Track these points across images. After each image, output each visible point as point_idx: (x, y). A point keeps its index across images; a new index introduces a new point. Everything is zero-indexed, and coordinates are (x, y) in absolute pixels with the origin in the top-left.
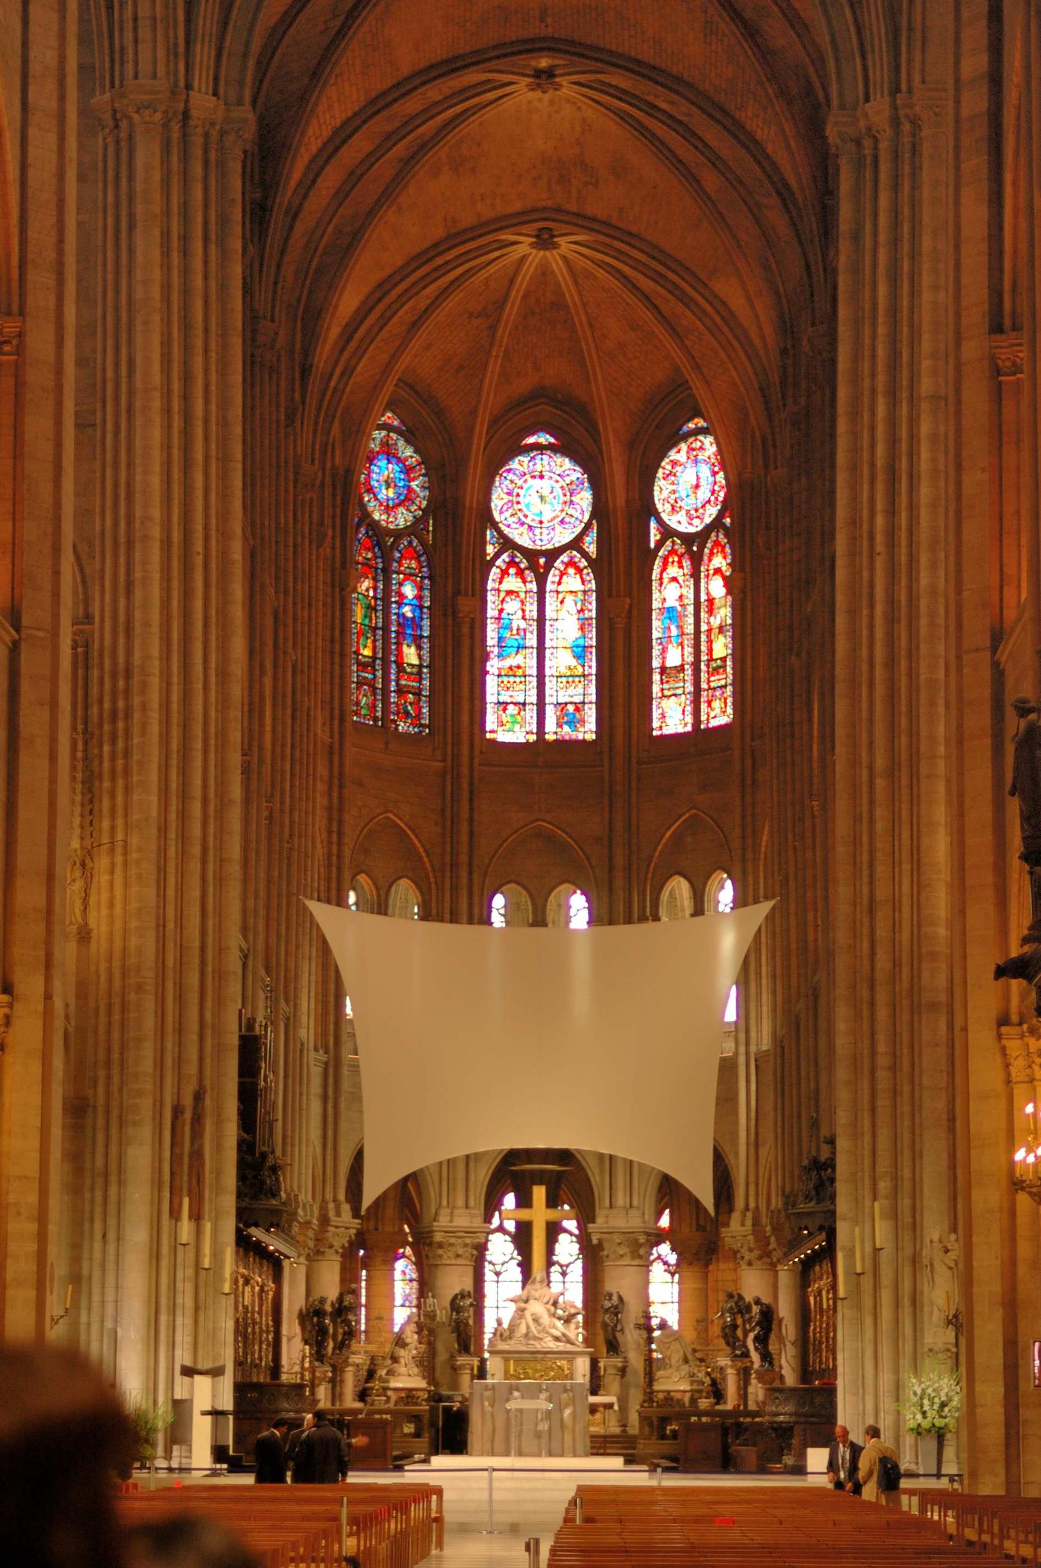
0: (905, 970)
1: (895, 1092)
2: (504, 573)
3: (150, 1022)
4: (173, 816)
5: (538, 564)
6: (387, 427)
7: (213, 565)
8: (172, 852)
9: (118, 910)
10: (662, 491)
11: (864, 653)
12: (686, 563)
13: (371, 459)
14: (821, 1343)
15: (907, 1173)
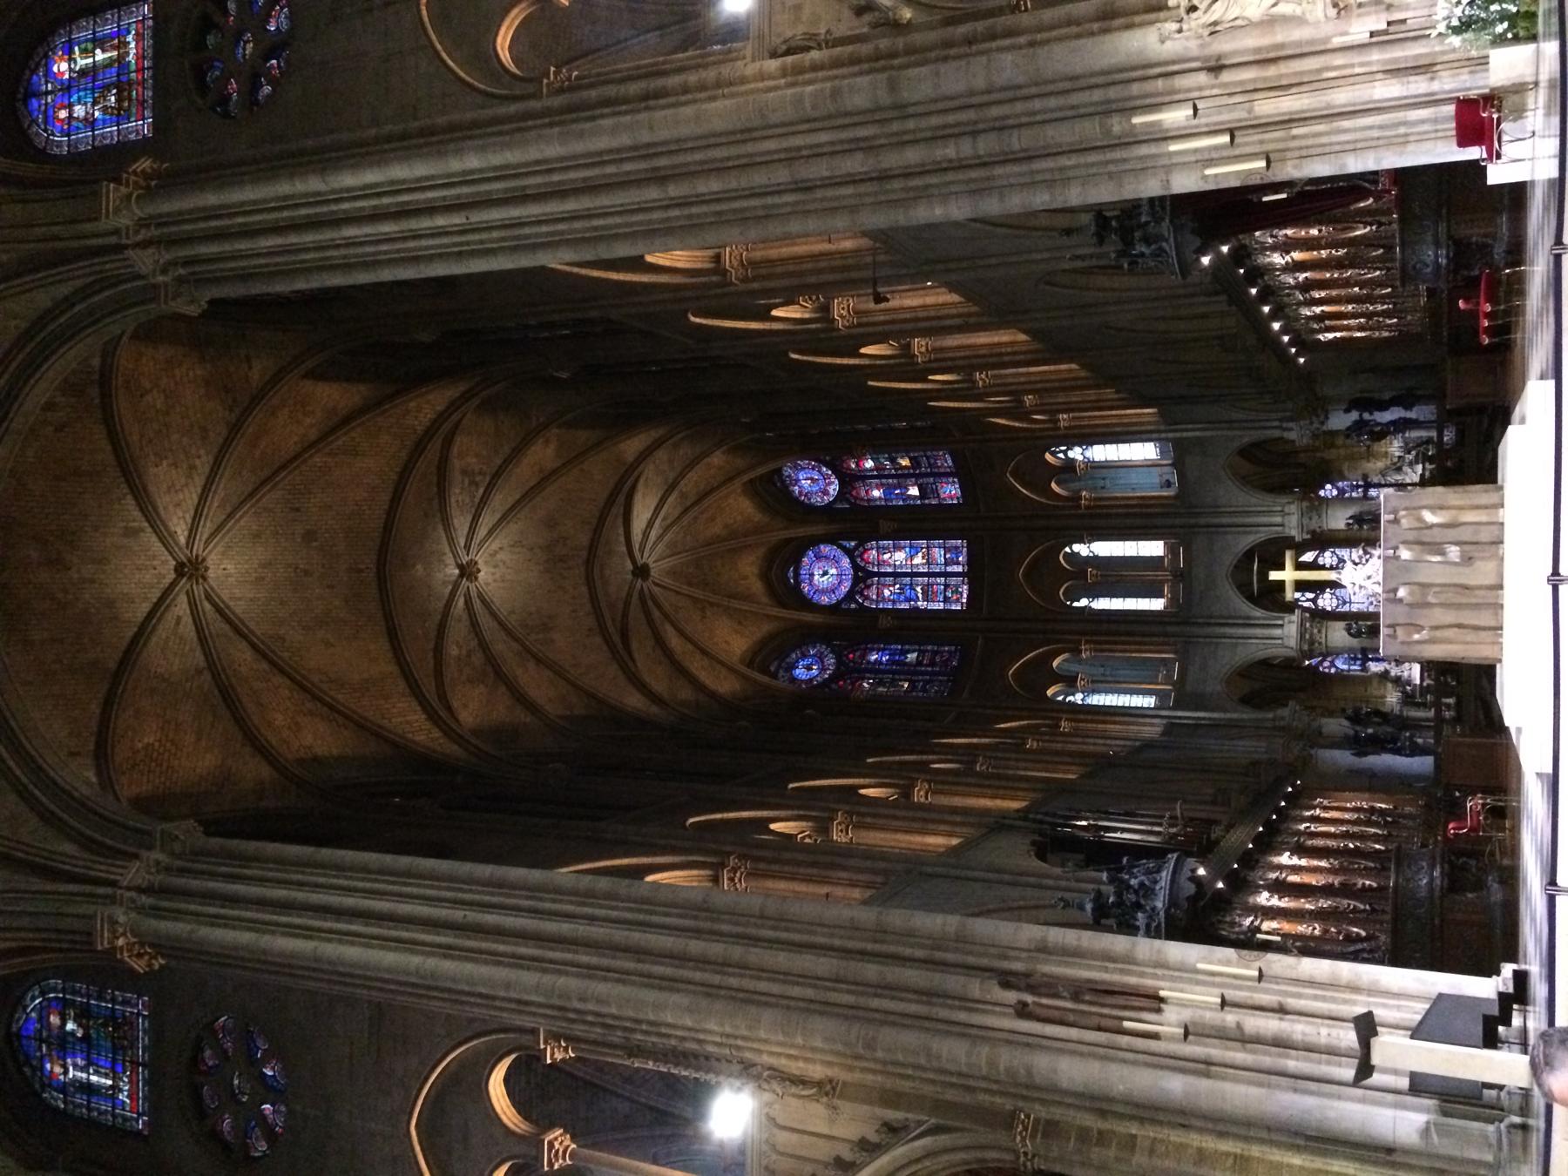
0: (862, 132)
1: (1001, 127)
2: (867, 598)
3: (910, 1038)
4: (698, 976)
5: (862, 576)
6: (779, 666)
7: (487, 898)
8: (734, 982)
9: (792, 1052)
10: (818, 500)
11: (561, 227)
12: (859, 484)
13: (793, 680)
14: (1369, 316)
15: (1097, 95)
